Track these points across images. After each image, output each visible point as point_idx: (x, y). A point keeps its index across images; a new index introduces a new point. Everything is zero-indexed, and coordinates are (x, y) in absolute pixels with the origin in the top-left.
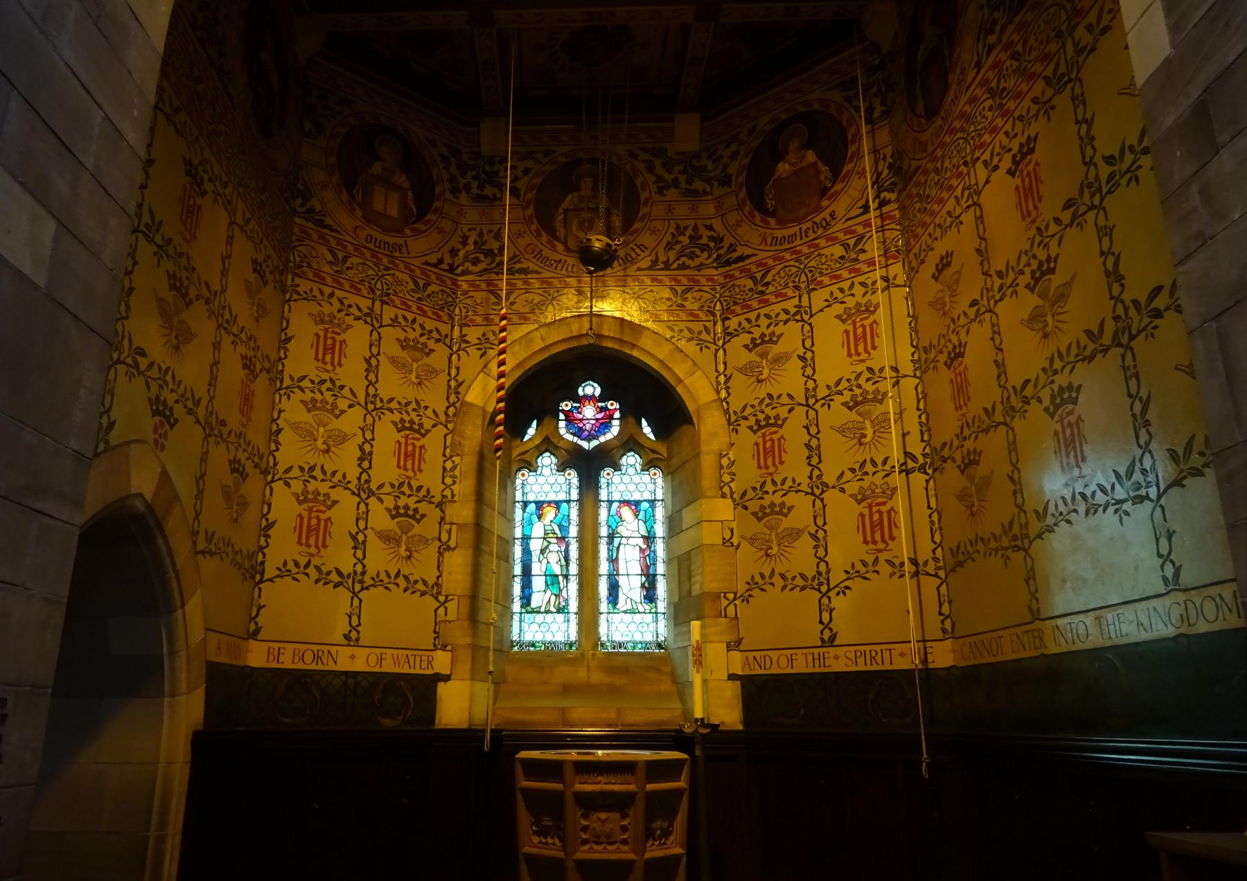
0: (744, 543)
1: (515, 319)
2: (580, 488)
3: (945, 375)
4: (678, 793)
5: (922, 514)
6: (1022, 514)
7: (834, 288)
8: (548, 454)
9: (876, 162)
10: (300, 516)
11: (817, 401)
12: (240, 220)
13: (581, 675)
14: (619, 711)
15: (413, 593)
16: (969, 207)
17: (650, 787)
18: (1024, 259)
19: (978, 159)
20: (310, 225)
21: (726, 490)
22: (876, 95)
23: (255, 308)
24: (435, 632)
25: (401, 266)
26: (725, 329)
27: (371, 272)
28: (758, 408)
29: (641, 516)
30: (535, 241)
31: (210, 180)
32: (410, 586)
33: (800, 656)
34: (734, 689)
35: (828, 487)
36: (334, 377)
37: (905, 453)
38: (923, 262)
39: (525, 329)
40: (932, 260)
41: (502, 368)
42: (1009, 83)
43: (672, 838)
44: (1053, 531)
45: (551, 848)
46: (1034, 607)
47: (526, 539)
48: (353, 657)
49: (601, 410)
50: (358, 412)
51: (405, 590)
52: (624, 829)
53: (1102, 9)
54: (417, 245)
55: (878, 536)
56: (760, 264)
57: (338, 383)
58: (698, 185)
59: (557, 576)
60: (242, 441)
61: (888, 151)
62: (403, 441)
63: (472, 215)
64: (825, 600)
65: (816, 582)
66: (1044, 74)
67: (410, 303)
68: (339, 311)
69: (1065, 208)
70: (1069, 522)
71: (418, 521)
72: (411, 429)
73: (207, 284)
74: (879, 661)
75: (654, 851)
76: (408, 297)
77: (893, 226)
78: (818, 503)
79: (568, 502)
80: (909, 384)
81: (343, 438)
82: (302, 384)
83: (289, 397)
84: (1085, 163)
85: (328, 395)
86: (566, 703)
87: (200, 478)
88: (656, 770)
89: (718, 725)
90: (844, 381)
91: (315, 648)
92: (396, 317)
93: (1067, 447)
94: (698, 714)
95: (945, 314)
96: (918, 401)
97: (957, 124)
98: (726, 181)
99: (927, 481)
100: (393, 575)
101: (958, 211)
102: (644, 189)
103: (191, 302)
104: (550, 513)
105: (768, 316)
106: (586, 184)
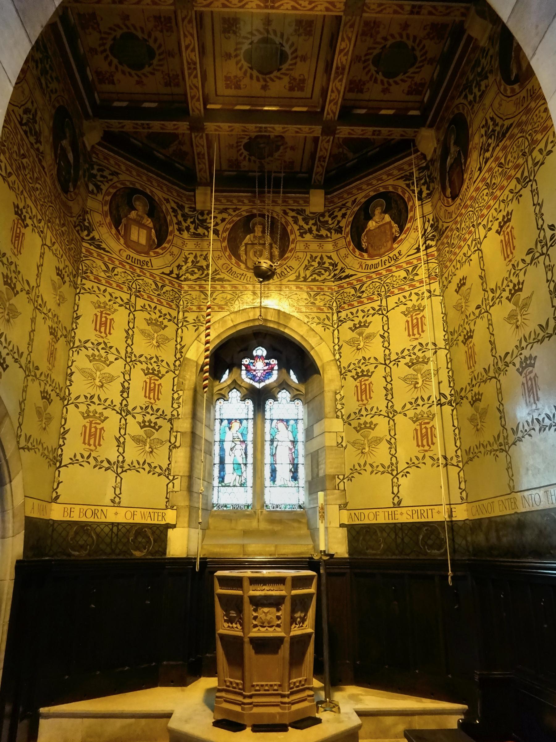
0: (349, 445)
1: (216, 308)
2: (254, 411)
3: (463, 348)
4: (310, 596)
5: (449, 429)
6: (505, 431)
7: (400, 296)
8: (235, 390)
9: (424, 224)
10: (85, 426)
11: (391, 362)
12: (48, 243)
14: (276, 546)
15: (154, 474)
16: (475, 251)
17: (294, 592)
18: (505, 282)
19: (480, 223)
20: (92, 247)
22: (424, 184)
23: (58, 298)
24: (167, 498)
25: (148, 274)
26: (339, 318)
27: (129, 277)
28: (357, 365)
29: (290, 428)
30: (229, 263)
31: (30, 218)
32: (152, 470)
33: (381, 512)
34: (343, 532)
35: (396, 412)
36: (106, 341)
37: (440, 393)
38: (450, 282)
39: (222, 314)
40: (456, 281)
41: (208, 338)
42: (497, 181)
43: (306, 623)
44: (522, 441)
45: (235, 630)
46: (511, 485)
47: (222, 442)
48: (116, 514)
49: (267, 364)
50: (121, 362)
51: (149, 472)
52: (278, 618)
53: (548, 139)
54: (157, 262)
55: (425, 442)
56: (358, 280)
57: (109, 345)
58: (323, 232)
59: (240, 464)
60: (49, 379)
61: (431, 217)
62: (148, 381)
63: (191, 245)
64: (395, 480)
65: (390, 469)
66: (516, 176)
67: (153, 297)
68: (110, 301)
69: (528, 254)
70: (530, 435)
71: (157, 430)
72: (153, 373)
73: (28, 282)
74: (426, 517)
75: (296, 631)
76: (151, 293)
77: (433, 260)
78: (391, 422)
79: (247, 419)
80: (442, 353)
81: (111, 379)
82: (87, 345)
83: (78, 353)
84: (538, 229)
85: (102, 352)
86: (245, 541)
87: (22, 403)
88: (298, 582)
89: (333, 555)
90: (406, 351)
91: (93, 508)
92: (144, 305)
93: (529, 392)
94: (322, 548)
95: (462, 313)
96: (448, 363)
97: (469, 203)
98: (339, 230)
99: (453, 410)
100: (141, 463)
101: (470, 253)
102: (292, 233)
103: (18, 292)
104: (236, 425)
105: (363, 311)
106: (258, 229)
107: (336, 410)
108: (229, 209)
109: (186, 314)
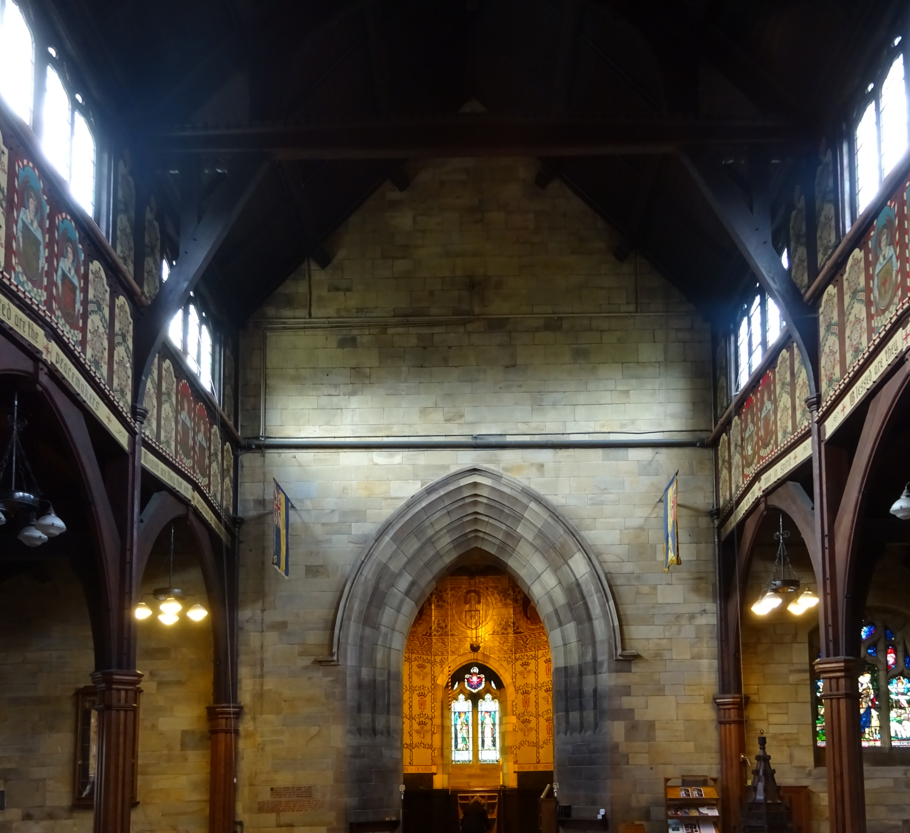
0: (519, 730)
13: (474, 771)
14: (484, 783)
21: (514, 713)
26: (515, 657)
34: (515, 776)
71: (425, 725)
107: (513, 711)
108: (455, 587)
109: (435, 657)
